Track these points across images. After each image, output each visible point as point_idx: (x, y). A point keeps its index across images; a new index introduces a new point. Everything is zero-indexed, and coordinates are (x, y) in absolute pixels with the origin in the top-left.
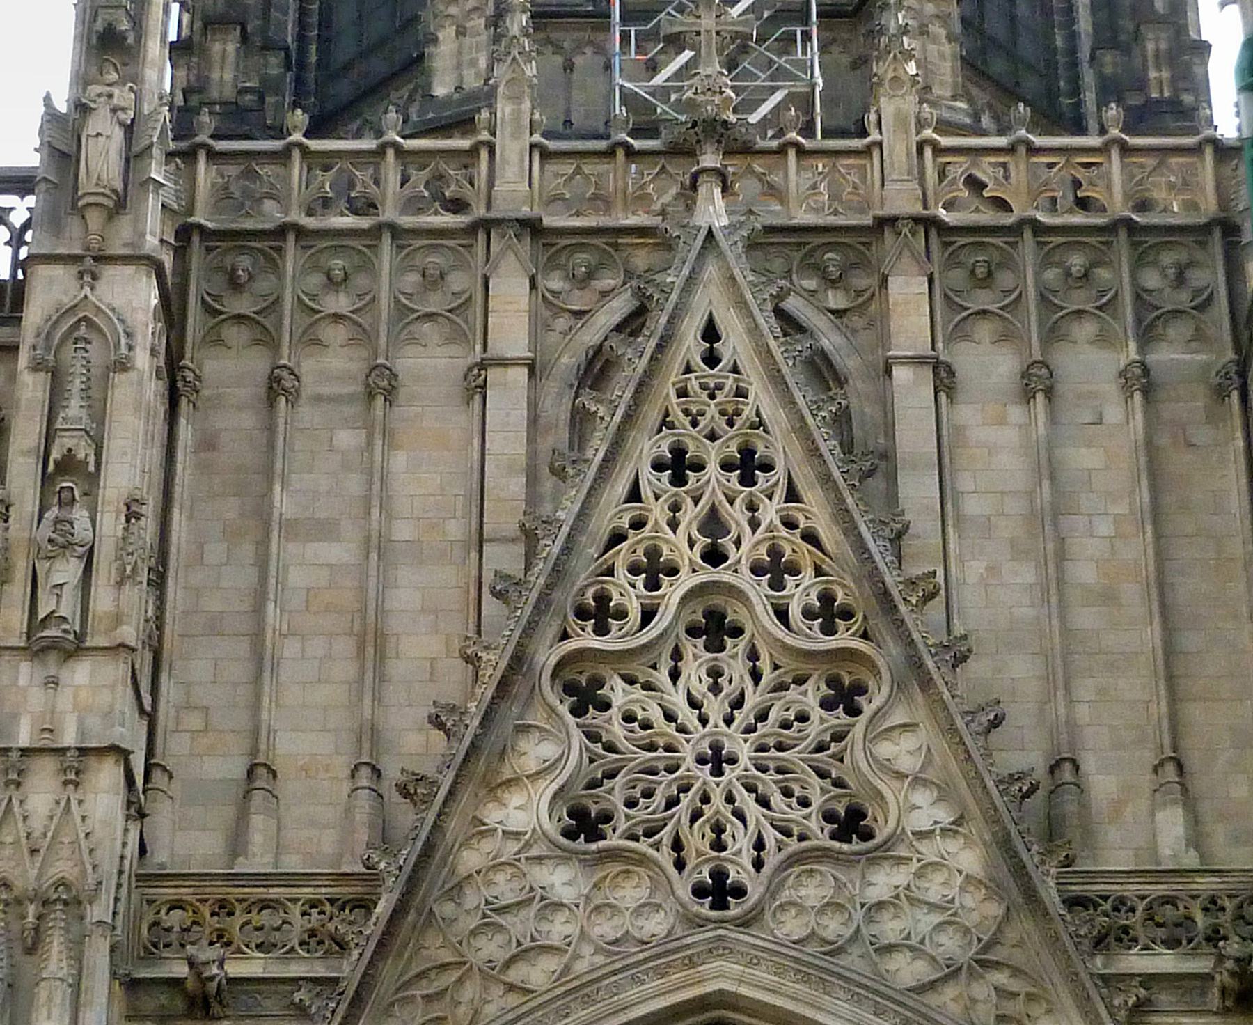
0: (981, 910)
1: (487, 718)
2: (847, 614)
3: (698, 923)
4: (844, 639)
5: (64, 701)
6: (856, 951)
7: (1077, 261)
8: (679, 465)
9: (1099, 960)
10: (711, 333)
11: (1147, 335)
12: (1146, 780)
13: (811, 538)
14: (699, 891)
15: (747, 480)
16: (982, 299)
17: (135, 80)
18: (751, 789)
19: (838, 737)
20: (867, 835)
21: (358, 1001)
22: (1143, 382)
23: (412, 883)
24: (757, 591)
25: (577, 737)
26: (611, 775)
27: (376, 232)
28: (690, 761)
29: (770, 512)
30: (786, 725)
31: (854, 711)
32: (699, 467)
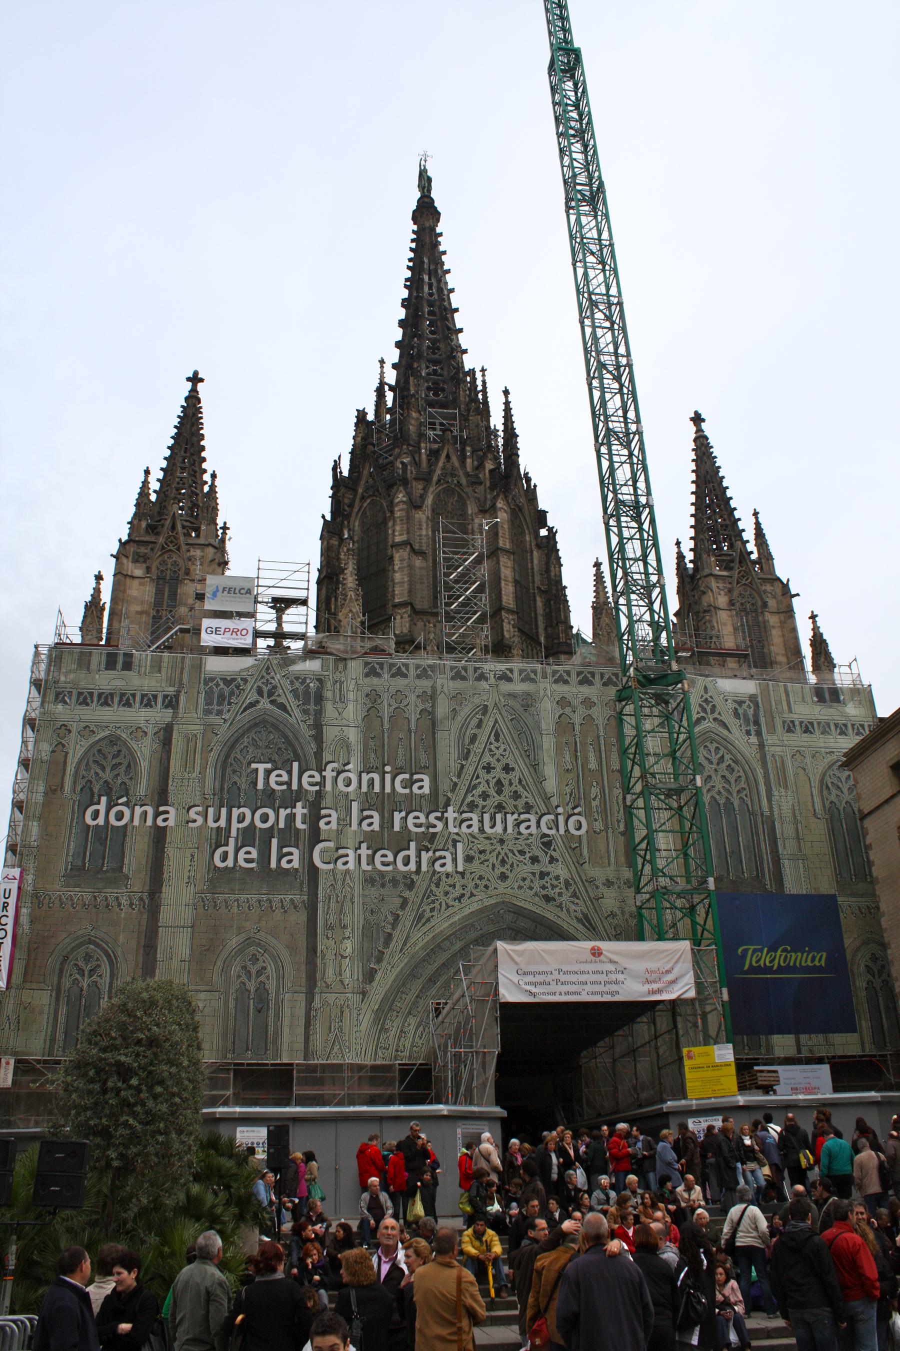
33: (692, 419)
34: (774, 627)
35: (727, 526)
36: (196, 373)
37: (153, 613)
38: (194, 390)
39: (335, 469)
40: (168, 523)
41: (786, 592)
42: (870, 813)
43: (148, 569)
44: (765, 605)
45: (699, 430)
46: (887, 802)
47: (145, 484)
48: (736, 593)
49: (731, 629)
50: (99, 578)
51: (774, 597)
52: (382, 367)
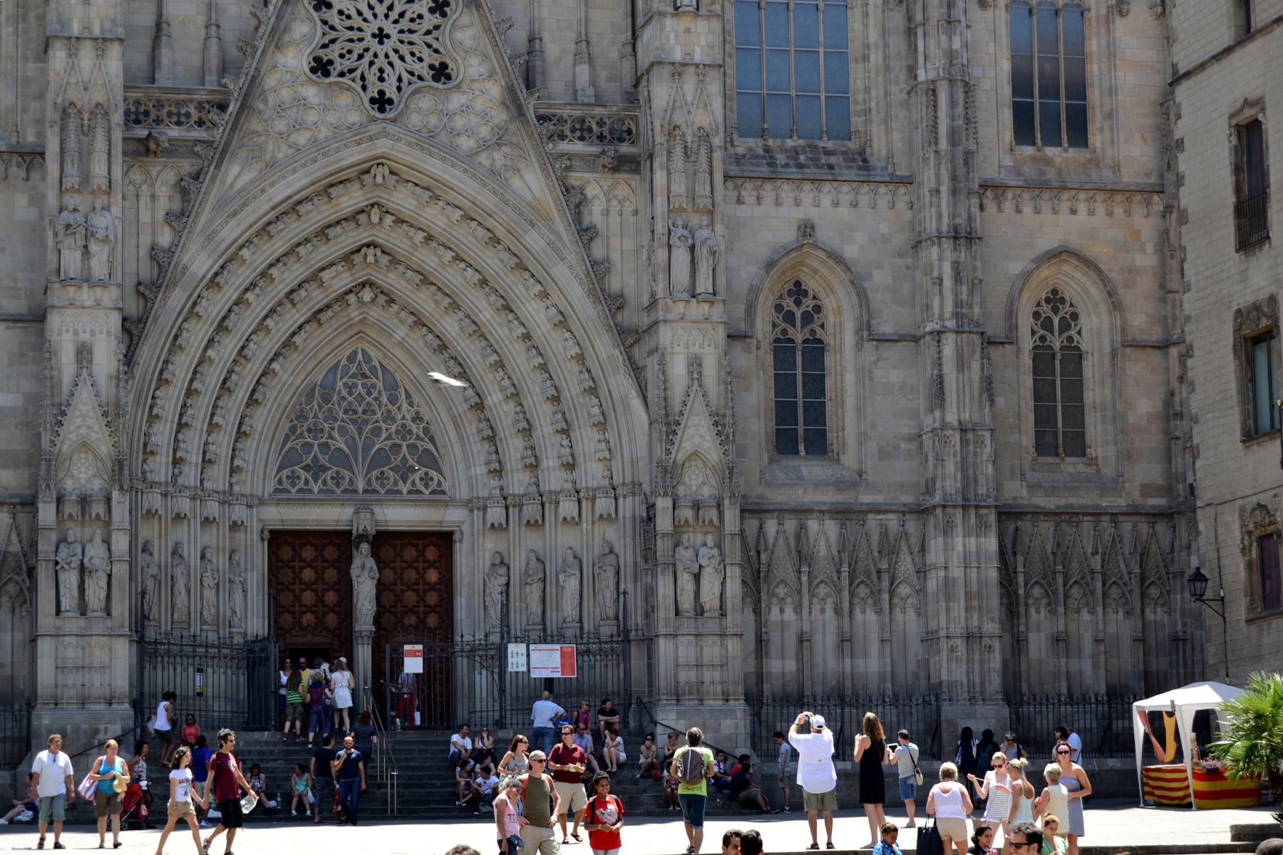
0: (500, 116)
1: (280, 16)
3: (374, 120)
5: (93, 12)
6: (443, 134)
9: (551, 145)
12: (572, 48)
14: (372, 101)
18: (396, 51)
19: (437, 27)
20: (449, 77)
21: (224, 152)
23: (247, 96)
25: (319, 23)
26: (333, 41)
28: (368, 37)
30: (412, 20)
31: (444, 15)
42: (1188, 75)
46: (1217, 57)
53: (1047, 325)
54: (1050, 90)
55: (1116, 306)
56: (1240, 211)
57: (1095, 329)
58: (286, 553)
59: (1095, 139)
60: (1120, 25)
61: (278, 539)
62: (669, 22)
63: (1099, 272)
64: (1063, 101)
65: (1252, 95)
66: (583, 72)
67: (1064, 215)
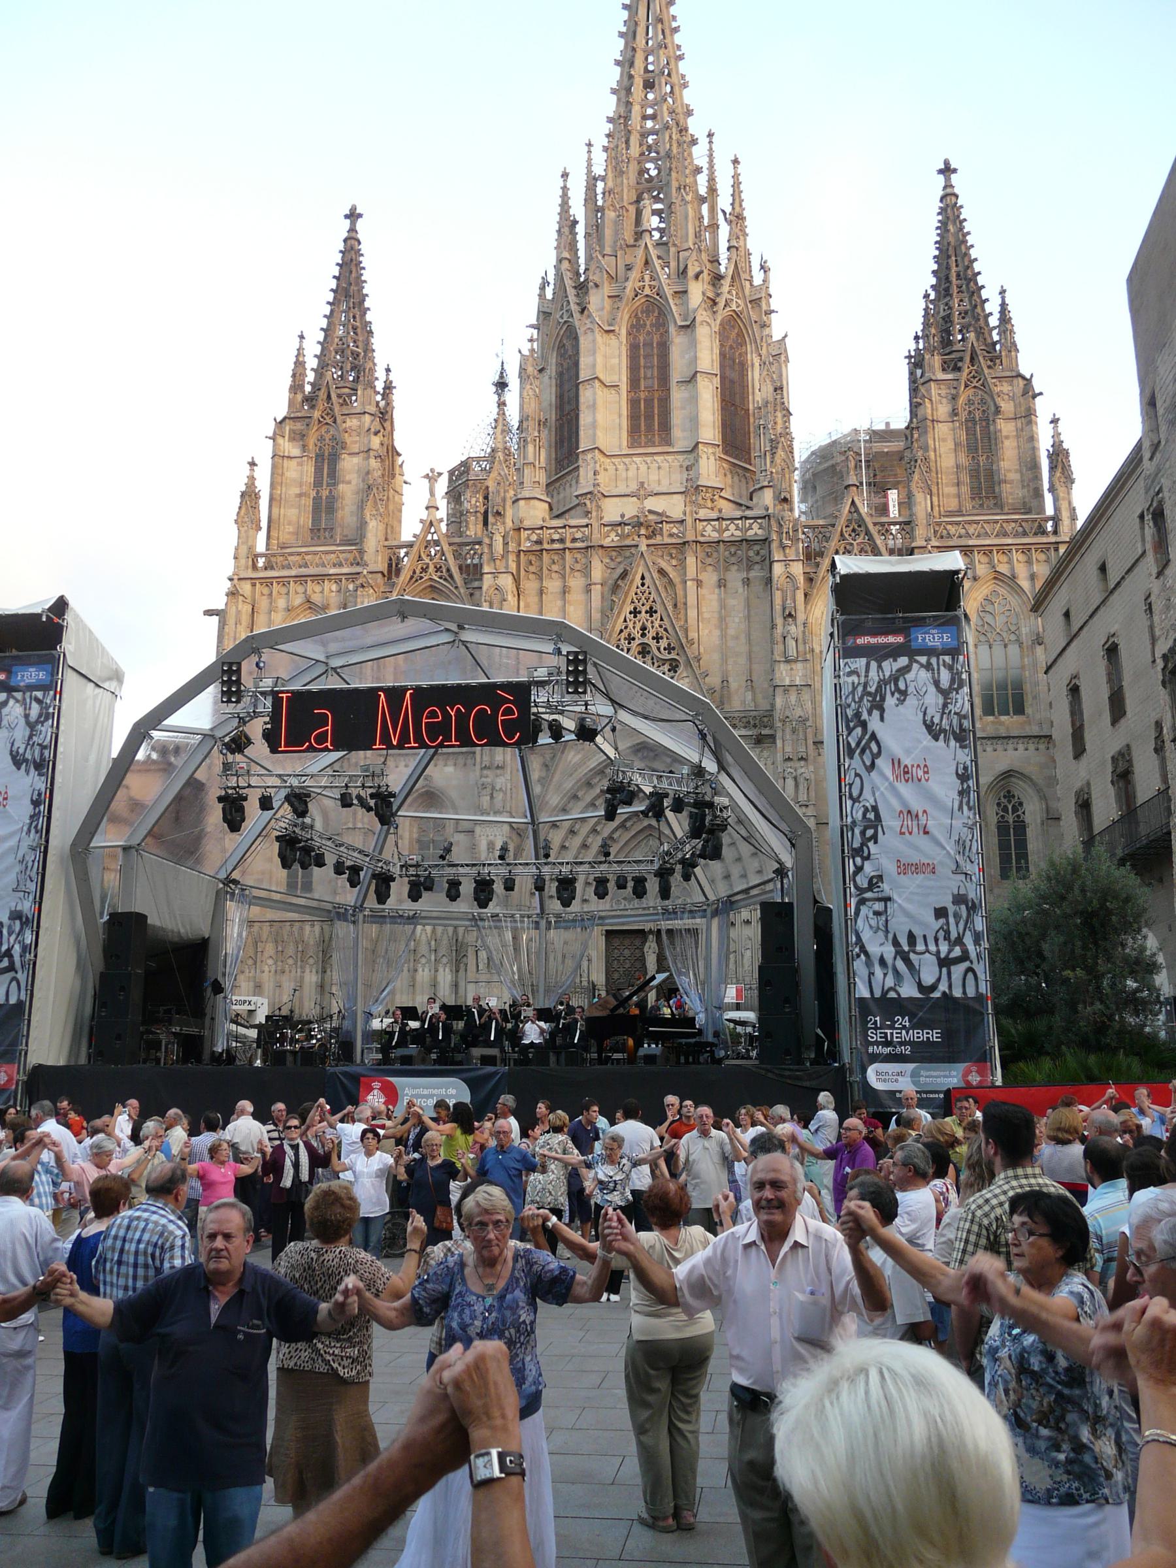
2: (674, 649)
4: (673, 656)
7: (733, 550)
8: (635, 612)
10: (643, 578)
11: (749, 569)
12: (744, 684)
13: (666, 630)
15: (651, 616)
16: (709, 561)
17: (504, 523)
22: (747, 582)
24: (653, 643)
27: (564, 549)
29: (656, 624)
32: (640, 612)
33: (941, 172)
34: (1007, 437)
35: (966, 313)
36: (353, 209)
37: (313, 494)
38: (353, 230)
39: (542, 288)
40: (322, 394)
41: (1028, 392)
43: (304, 446)
44: (998, 410)
45: (949, 185)
47: (300, 352)
48: (962, 400)
49: (950, 444)
50: (253, 464)
51: (1013, 399)
52: (589, 152)
53: (1005, 810)
54: (1002, 686)
55: (1043, 798)
56: (1073, 735)
57: (1032, 812)
58: (616, 942)
59: (1029, 710)
60: (1039, 650)
61: (609, 934)
62: (782, 666)
63: (1031, 780)
64: (1010, 692)
65: (1075, 673)
66: (749, 695)
67: (1010, 752)
